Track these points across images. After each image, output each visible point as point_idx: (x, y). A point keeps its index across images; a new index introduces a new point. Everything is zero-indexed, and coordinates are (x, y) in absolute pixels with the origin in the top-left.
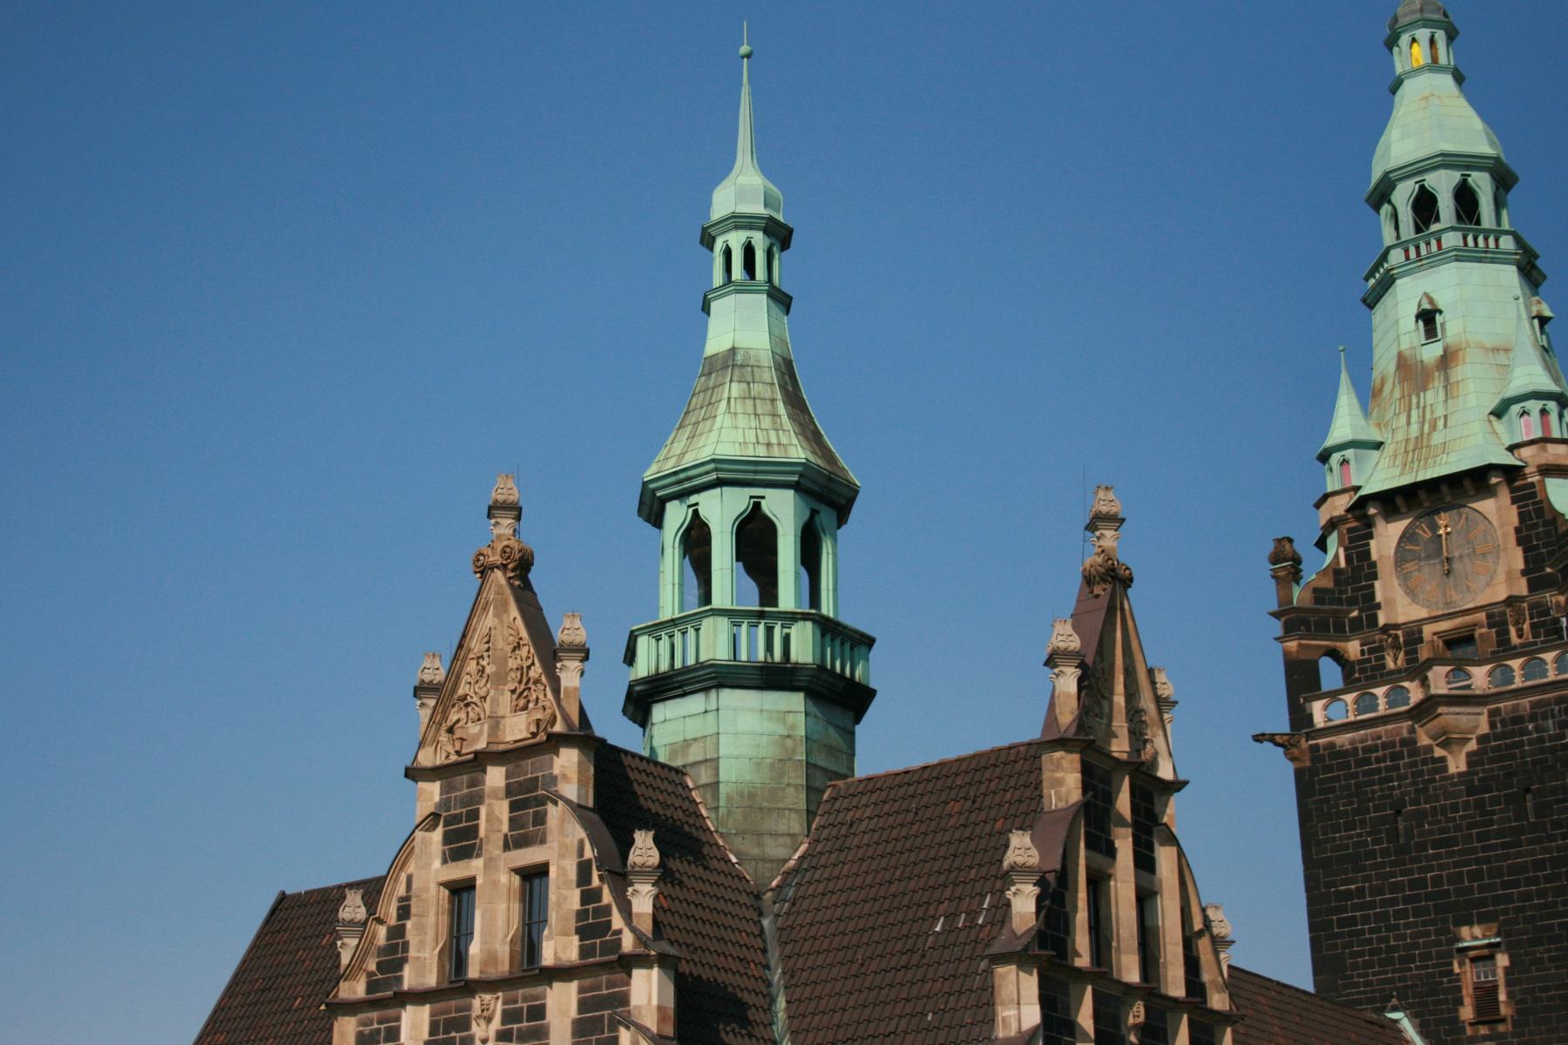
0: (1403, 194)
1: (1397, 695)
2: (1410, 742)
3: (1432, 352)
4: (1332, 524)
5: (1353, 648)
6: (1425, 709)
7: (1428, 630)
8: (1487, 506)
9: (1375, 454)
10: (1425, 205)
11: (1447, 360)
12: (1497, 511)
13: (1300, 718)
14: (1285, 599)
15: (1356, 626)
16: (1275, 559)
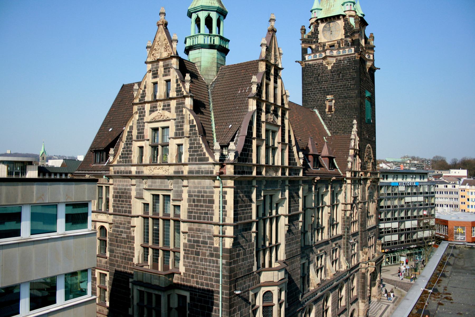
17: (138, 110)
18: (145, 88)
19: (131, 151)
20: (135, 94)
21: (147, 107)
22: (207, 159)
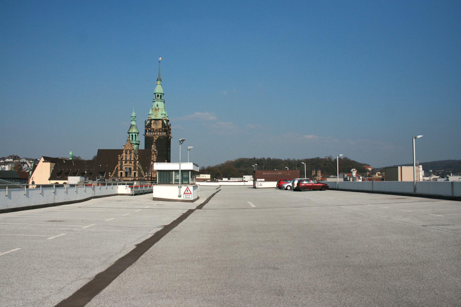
0: (157, 95)
1: (152, 134)
2: (153, 137)
3: (157, 108)
4: (149, 120)
5: (149, 129)
6: (155, 135)
7: (155, 129)
8: (160, 121)
9: (152, 115)
10: (158, 96)
11: (158, 109)
12: (161, 122)
13: (146, 134)
14: (145, 125)
15: (150, 127)
16: (145, 122)
17: (120, 162)
18: (123, 156)
19: (118, 173)
20: (119, 158)
21: (124, 162)
22: (144, 176)
